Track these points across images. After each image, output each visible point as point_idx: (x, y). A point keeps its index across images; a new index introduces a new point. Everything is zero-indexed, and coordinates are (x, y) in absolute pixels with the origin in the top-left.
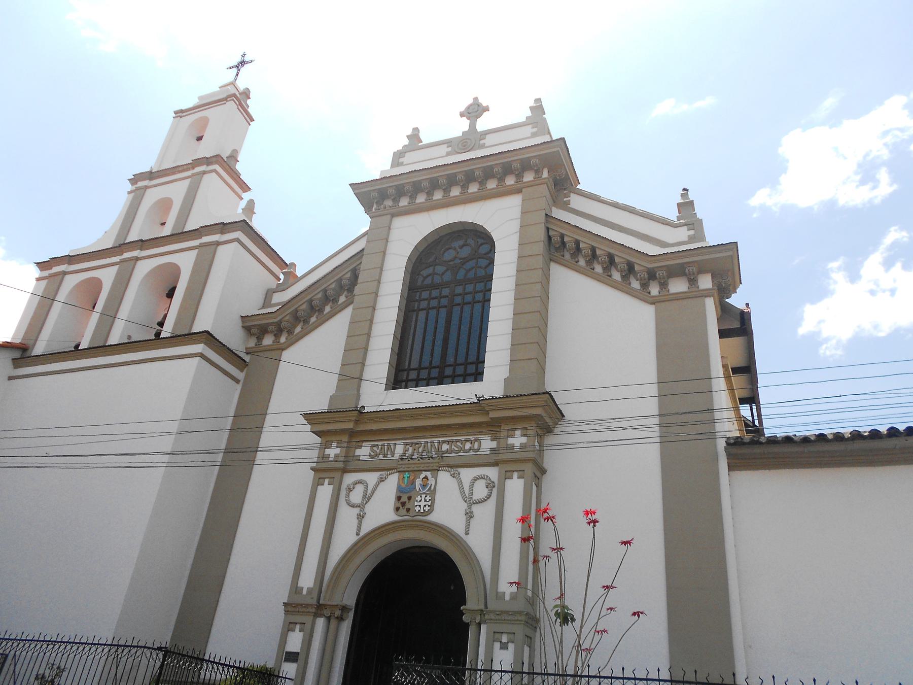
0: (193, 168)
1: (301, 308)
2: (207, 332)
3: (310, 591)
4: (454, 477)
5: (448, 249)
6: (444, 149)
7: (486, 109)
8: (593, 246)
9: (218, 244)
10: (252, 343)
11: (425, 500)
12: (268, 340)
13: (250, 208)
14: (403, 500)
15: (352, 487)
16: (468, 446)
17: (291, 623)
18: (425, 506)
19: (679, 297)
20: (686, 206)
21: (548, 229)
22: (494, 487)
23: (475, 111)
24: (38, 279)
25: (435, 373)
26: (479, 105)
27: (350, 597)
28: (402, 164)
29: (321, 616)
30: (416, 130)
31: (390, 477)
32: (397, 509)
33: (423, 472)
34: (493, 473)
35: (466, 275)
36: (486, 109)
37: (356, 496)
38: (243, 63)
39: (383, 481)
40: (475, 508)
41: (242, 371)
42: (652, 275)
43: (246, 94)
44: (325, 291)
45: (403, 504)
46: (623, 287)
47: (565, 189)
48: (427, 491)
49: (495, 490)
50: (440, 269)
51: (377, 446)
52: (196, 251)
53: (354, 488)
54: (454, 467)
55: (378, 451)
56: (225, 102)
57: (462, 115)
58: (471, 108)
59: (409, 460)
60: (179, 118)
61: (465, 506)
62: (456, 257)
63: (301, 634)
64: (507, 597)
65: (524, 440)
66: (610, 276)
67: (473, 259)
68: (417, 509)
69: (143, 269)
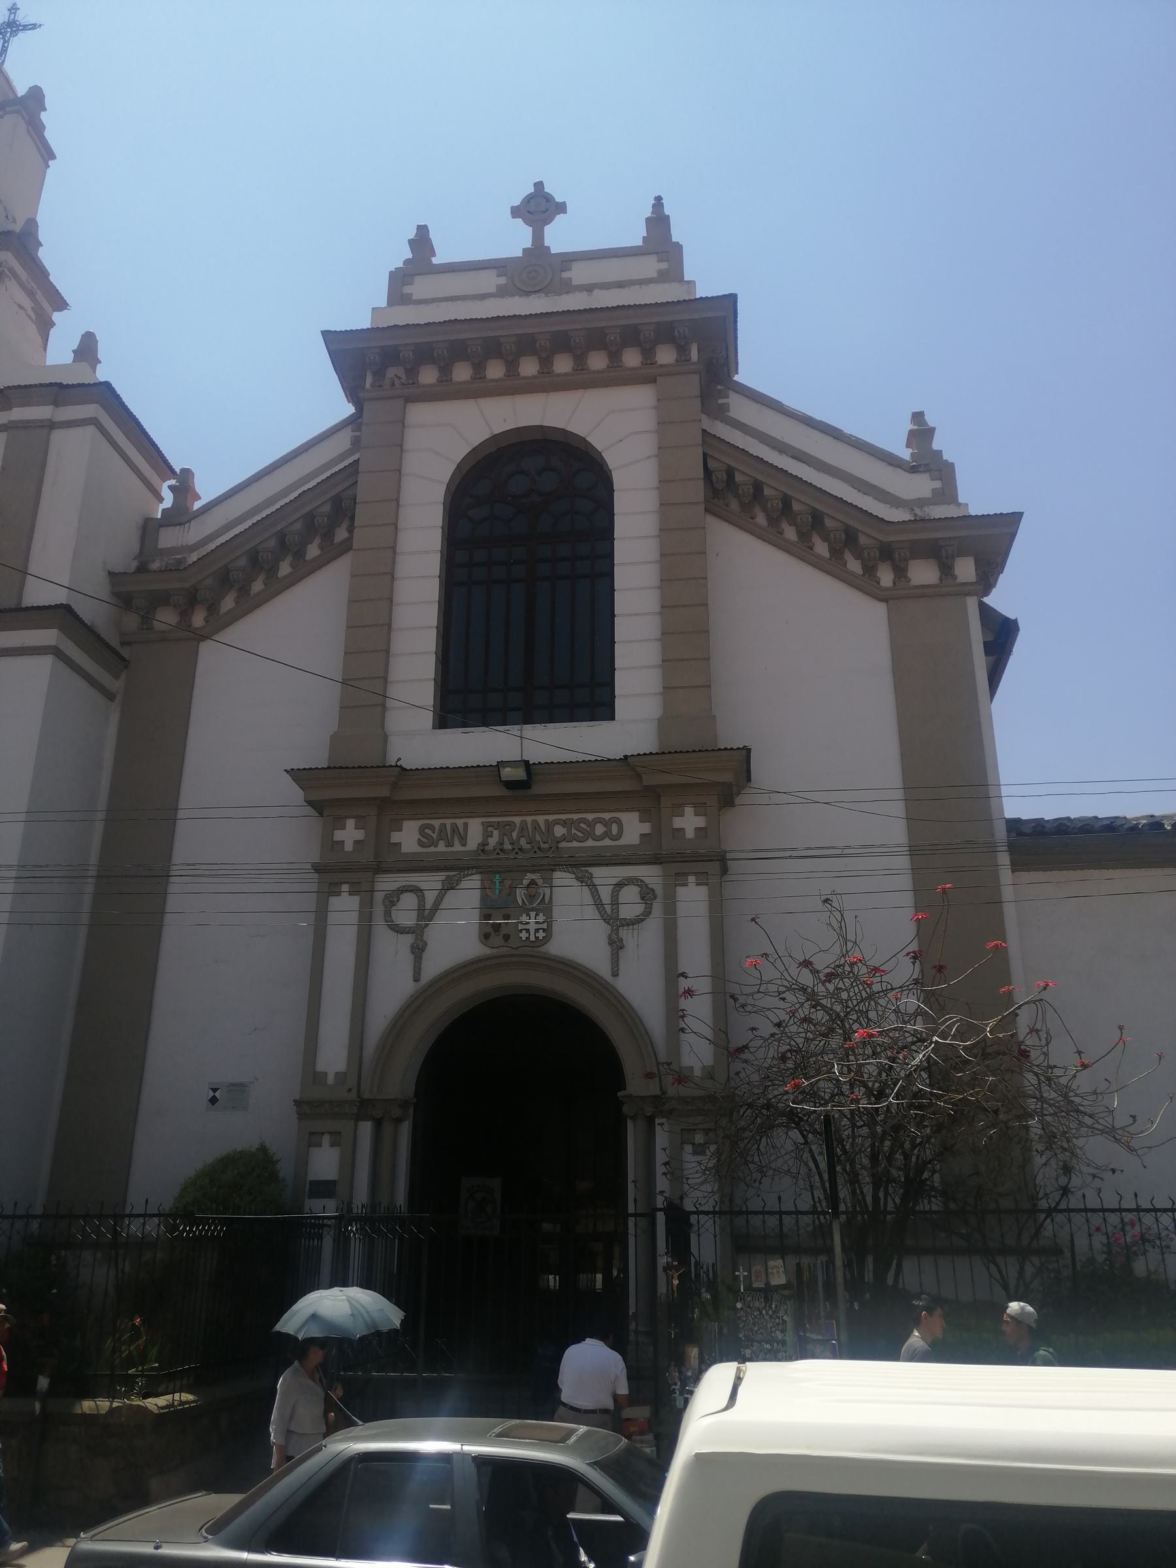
2: (66, 609)
3: (341, 1077)
4: (582, 882)
7: (561, 208)
9: (52, 425)
10: (131, 621)
12: (166, 618)
13: (87, 349)
15: (395, 899)
16: (600, 829)
17: (314, 1133)
18: (537, 931)
19: (924, 593)
20: (921, 433)
21: (705, 456)
22: (655, 898)
26: (548, 198)
30: (423, 230)
31: (464, 884)
32: (485, 937)
33: (528, 874)
34: (650, 874)
36: (561, 208)
37: (406, 914)
40: (624, 933)
41: (117, 677)
42: (887, 553)
46: (833, 567)
48: (538, 904)
49: (657, 907)
53: (398, 901)
54: (580, 865)
55: (435, 836)
57: (516, 212)
58: (532, 201)
59: (498, 854)
65: (700, 822)
66: (811, 548)
68: (524, 935)
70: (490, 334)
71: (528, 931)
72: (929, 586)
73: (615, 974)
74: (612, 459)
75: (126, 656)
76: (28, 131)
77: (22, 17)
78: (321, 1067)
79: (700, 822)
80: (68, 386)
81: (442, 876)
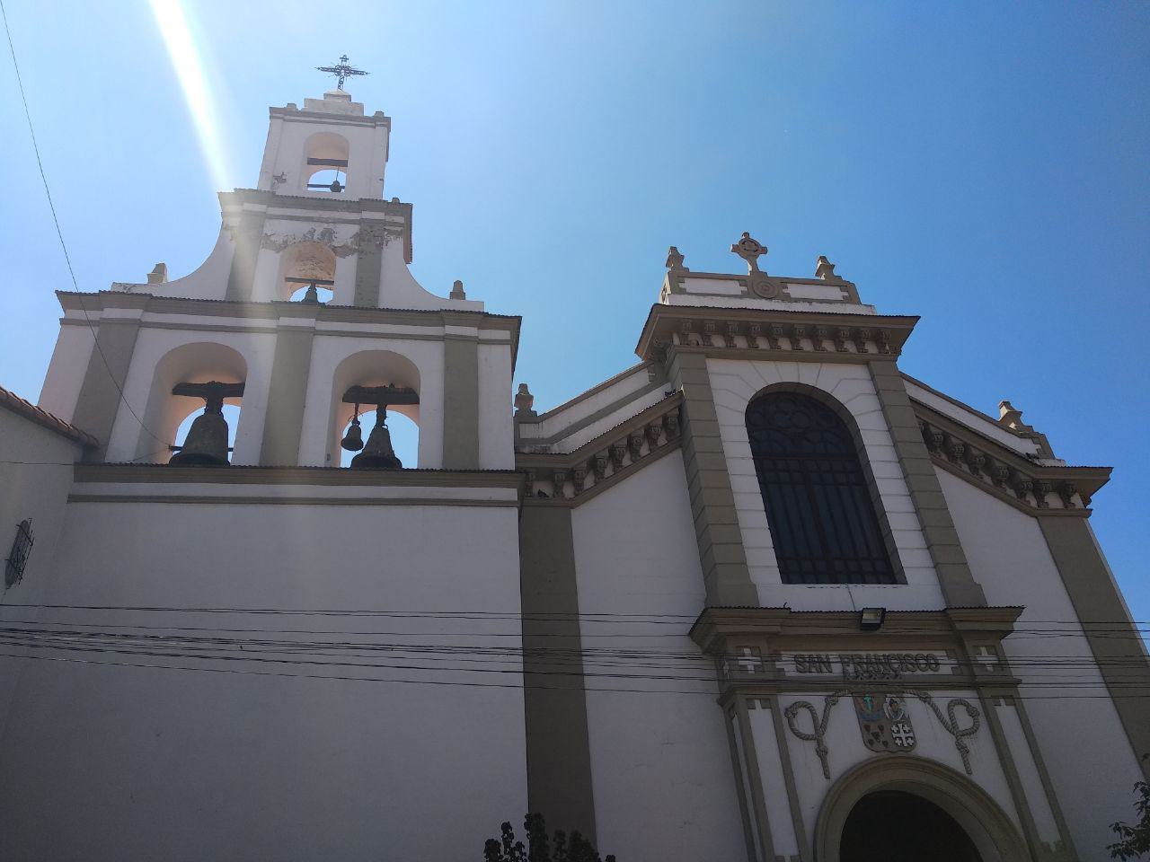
4: (925, 702)
6: (735, 288)
7: (765, 251)
8: (966, 443)
11: (905, 731)
13: (458, 292)
18: (907, 738)
19: (1055, 514)
20: (1014, 415)
26: (756, 244)
28: (683, 292)
30: (673, 249)
32: (871, 742)
34: (969, 695)
37: (804, 723)
39: (834, 704)
40: (966, 741)
45: (876, 736)
51: (803, 658)
52: (440, 346)
54: (922, 689)
57: (736, 249)
64: (1053, 848)
65: (993, 659)
70: (767, 320)
71: (900, 738)
73: (969, 772)
74: (853, 408)
78: (778, 851)
79: (993, 659)
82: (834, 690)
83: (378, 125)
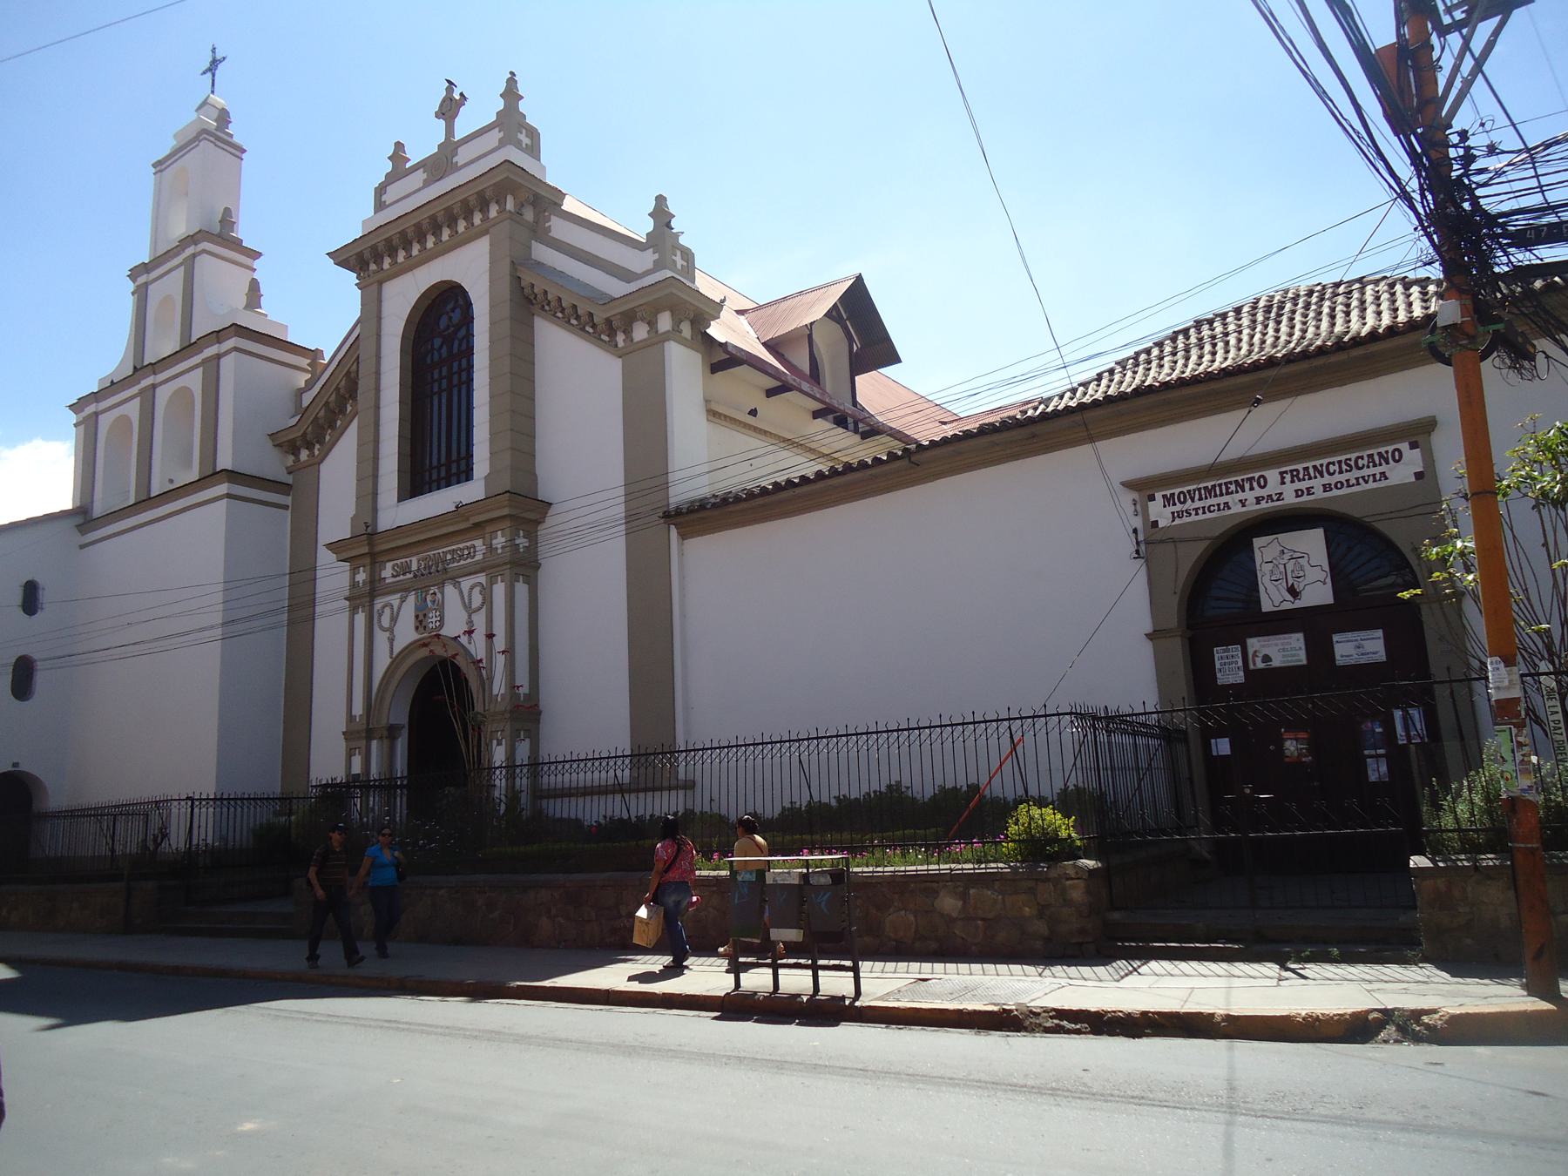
0: (183, 250)
1: (320, 414)
5: (441, 316)
6: (420, 176)
10: (291, 458)
12: (304, 455)
14: (420, 619)
16: (466, 552)
19: (645, 345)
23: (450, 108)
24: (75, 425)
25: (443, 469)
27: (400, 715)
29: (374, 739)
30: (399, 146)
32: (417, 628)
34: (482, 578)
35: (460, 345)
38: (215, 63)
41: (289, 495)
43: (224, 117)
44: (337, 389)
45: (421, 622)
47: (545, 211)
50: (437, 342)
56: (197, 143)
60: (159, 174)
61: (465, 616)
62: (448, 327)
63: (360, 757)
67: (462, 327)
68: (431, 625)
69: (163, 395)
72: (645, 340)
73: (470, 643)
75: (290, 482)
76: (216, 145)
77: (218, 57)
80: (220, 331)
81: (398, 596)
82: (404, 589)
83: (200, 142)
